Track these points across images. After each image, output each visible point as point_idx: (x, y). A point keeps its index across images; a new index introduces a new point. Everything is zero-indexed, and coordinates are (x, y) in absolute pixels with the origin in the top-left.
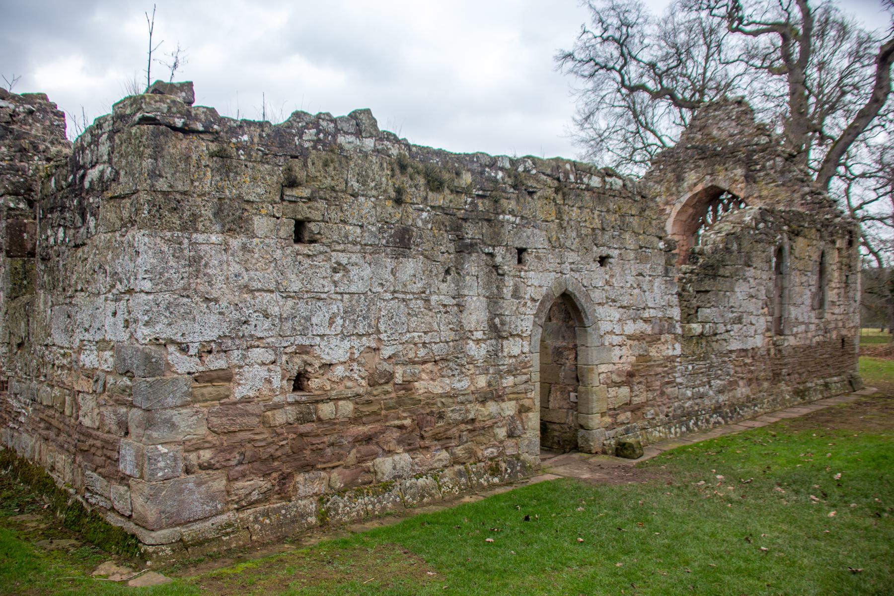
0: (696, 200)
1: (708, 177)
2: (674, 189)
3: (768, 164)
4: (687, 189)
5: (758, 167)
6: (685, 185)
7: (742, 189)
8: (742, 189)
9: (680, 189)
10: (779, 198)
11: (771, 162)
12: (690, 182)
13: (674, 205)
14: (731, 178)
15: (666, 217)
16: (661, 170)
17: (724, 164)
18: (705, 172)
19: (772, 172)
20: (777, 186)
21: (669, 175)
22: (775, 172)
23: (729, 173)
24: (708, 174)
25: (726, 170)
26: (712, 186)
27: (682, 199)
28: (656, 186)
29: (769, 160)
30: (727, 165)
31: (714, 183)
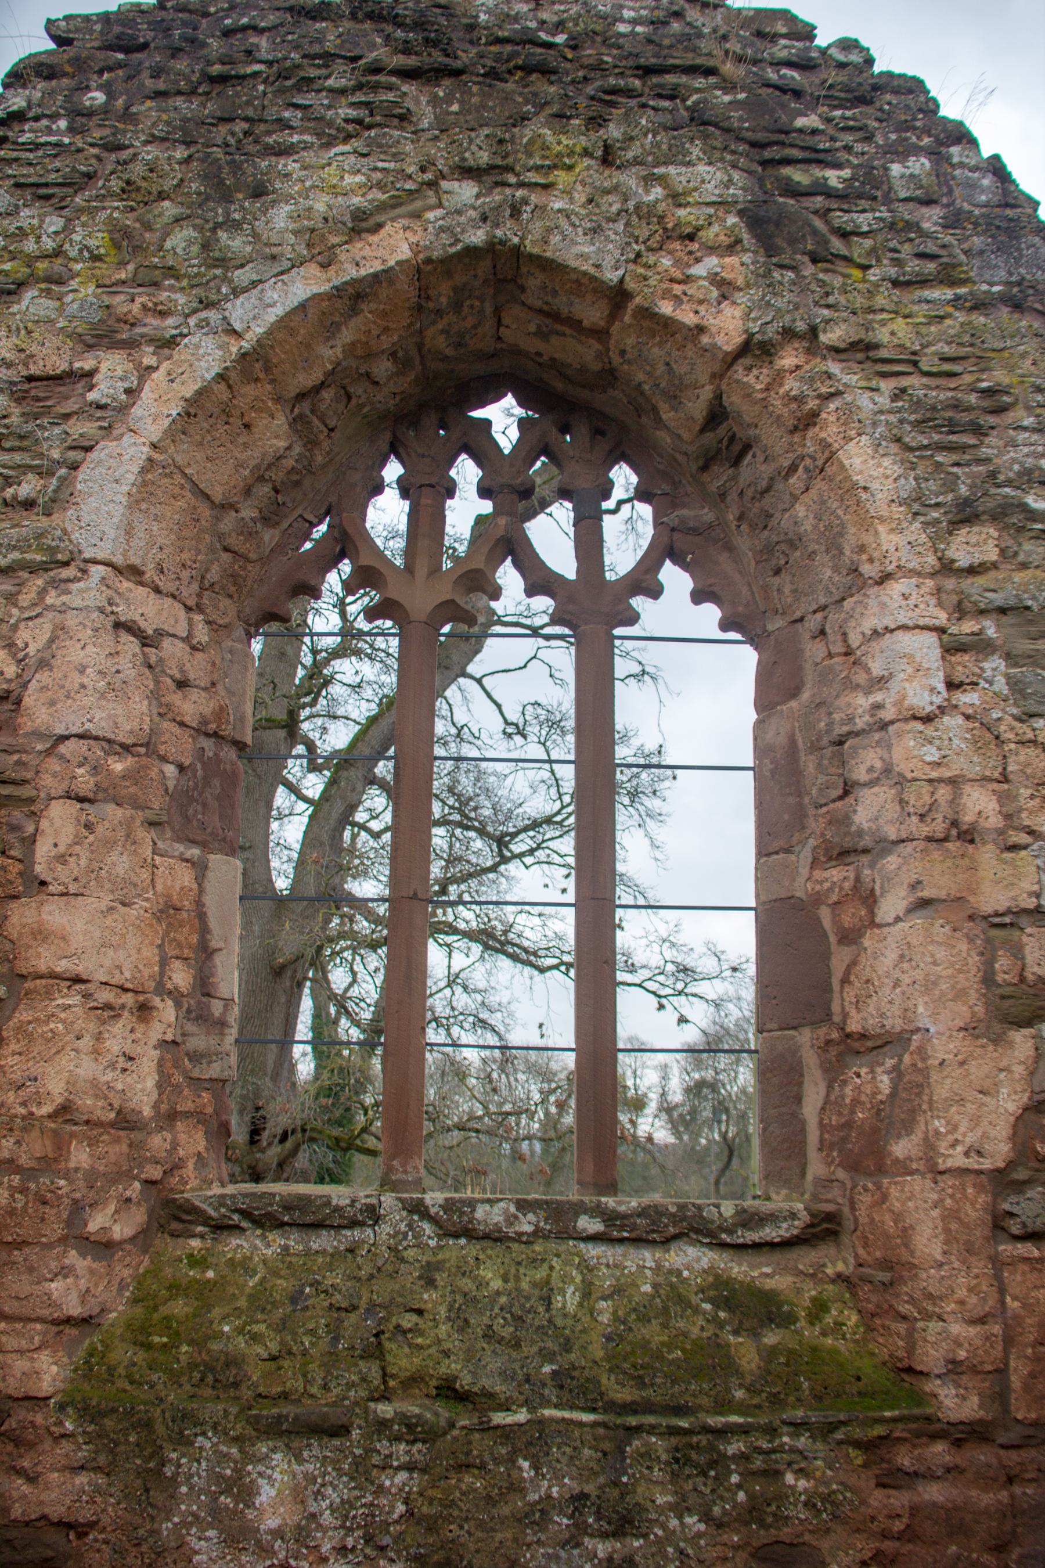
0: (329, 353)
1: (466, 191)
2: (180, 239)
3: (896, 169)
4: (291, 247)
5: (834, 178)
6: (281, 217)
7: (725, 288)
8: (725, 288)
9: (236, 243)
10: (1000, 376)
11: (920, 165)
12: (320, 204)
13: (168, 344)
14: (646, 213)
15: (78, 428)
16: (79, 115)
17: (596, 122)
18: (441, 155)
19: (930, 218)
20: (980, 305)
21: (151, 153)
22: (954, 221)
23: (630, 180)
24: (468, 172)
25: (608, 158)
26: (492, 249)
27: (238, 311)
28: (27, 217)
29: (902, 152)
30: (614, 131)
31: (507, 232)
